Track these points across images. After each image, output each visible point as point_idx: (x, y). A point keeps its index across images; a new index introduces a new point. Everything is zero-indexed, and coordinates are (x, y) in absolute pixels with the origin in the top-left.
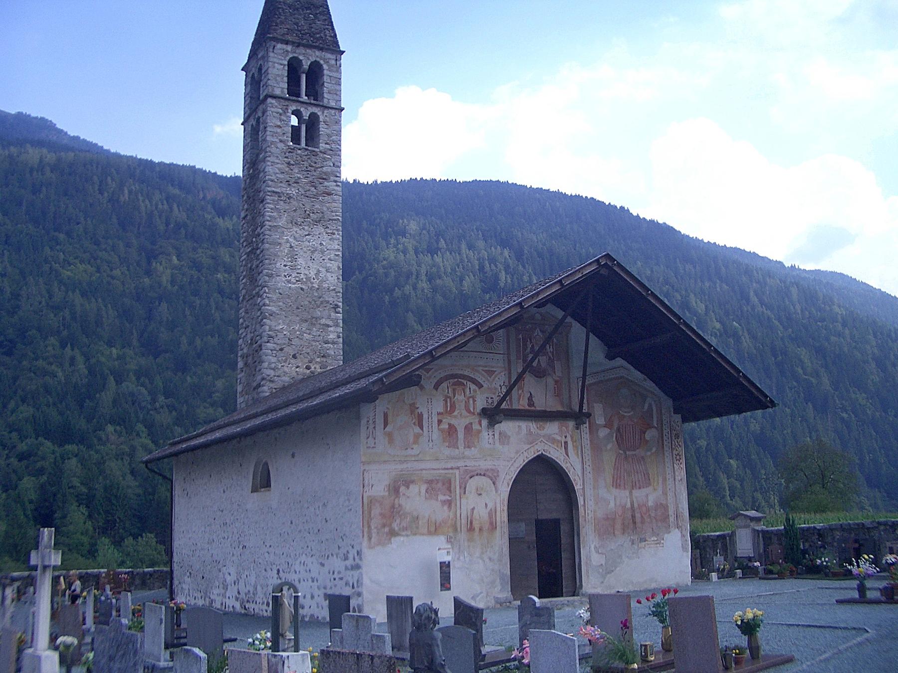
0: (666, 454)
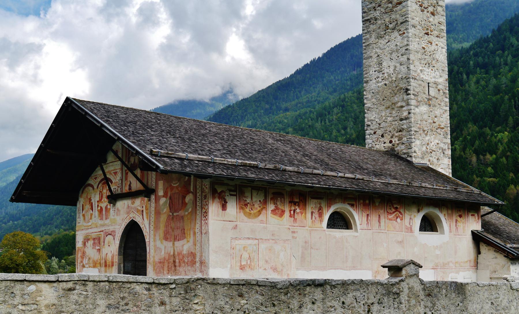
0: (198, 212)
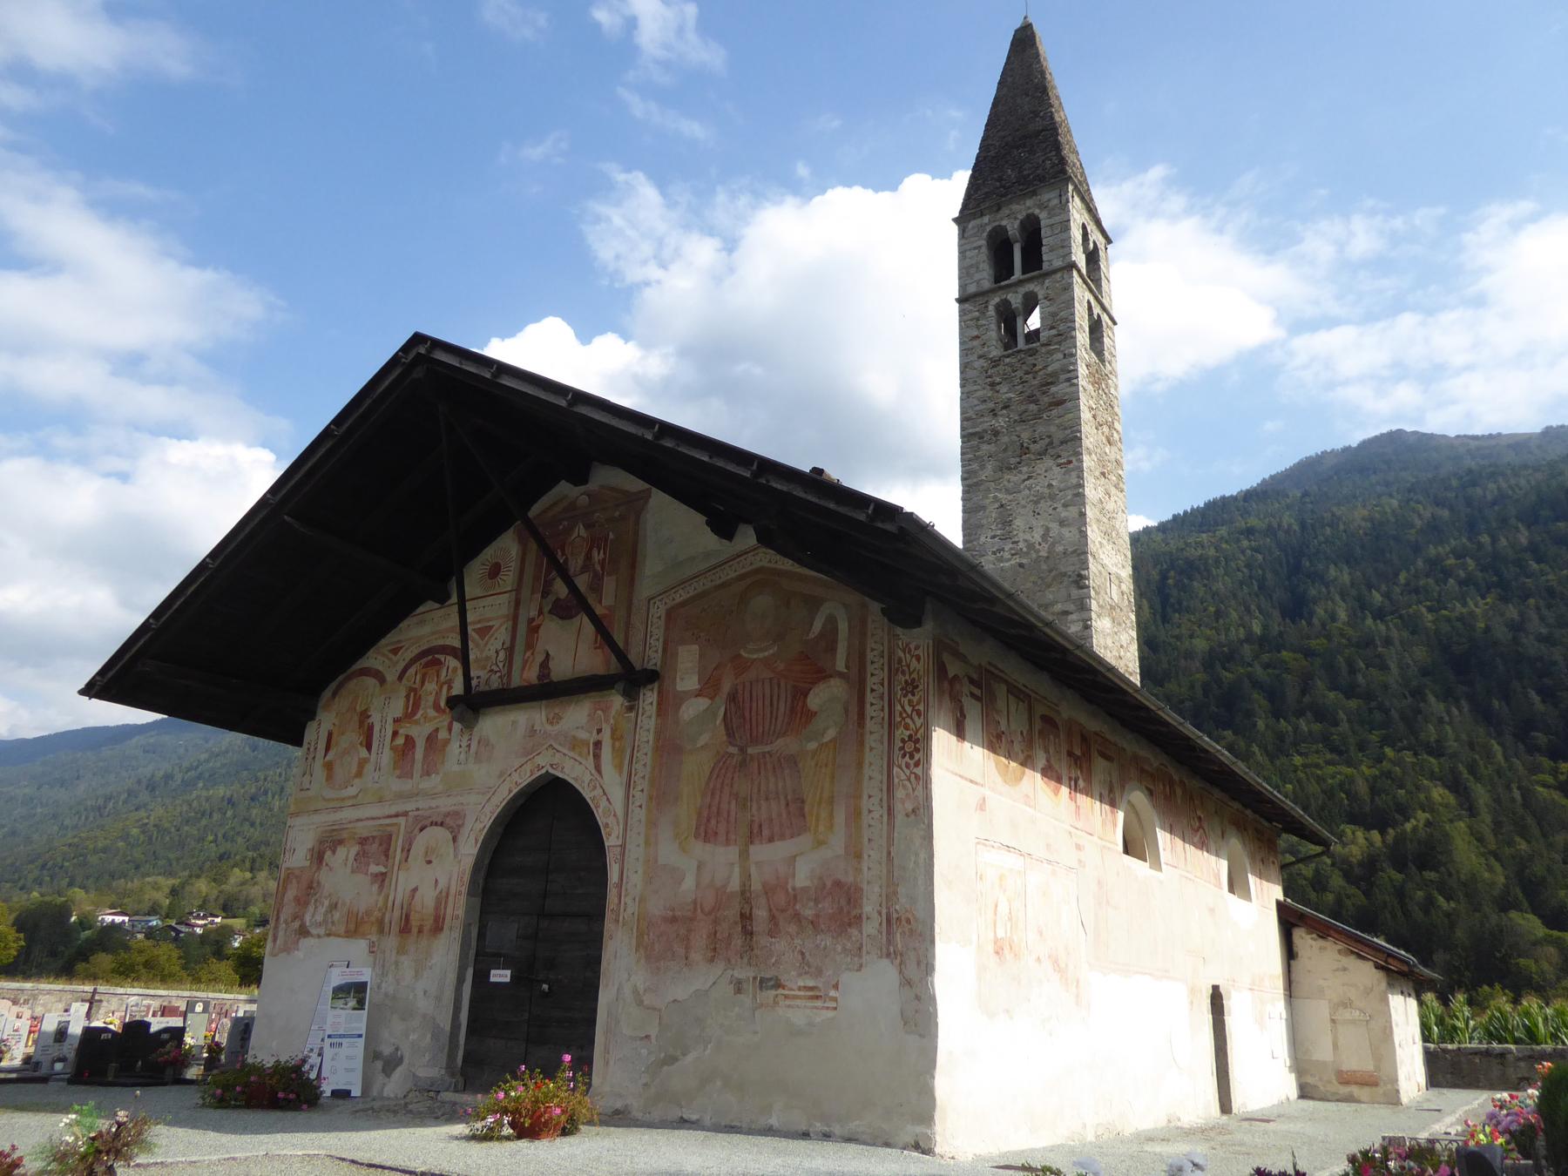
0: (870, 740)
